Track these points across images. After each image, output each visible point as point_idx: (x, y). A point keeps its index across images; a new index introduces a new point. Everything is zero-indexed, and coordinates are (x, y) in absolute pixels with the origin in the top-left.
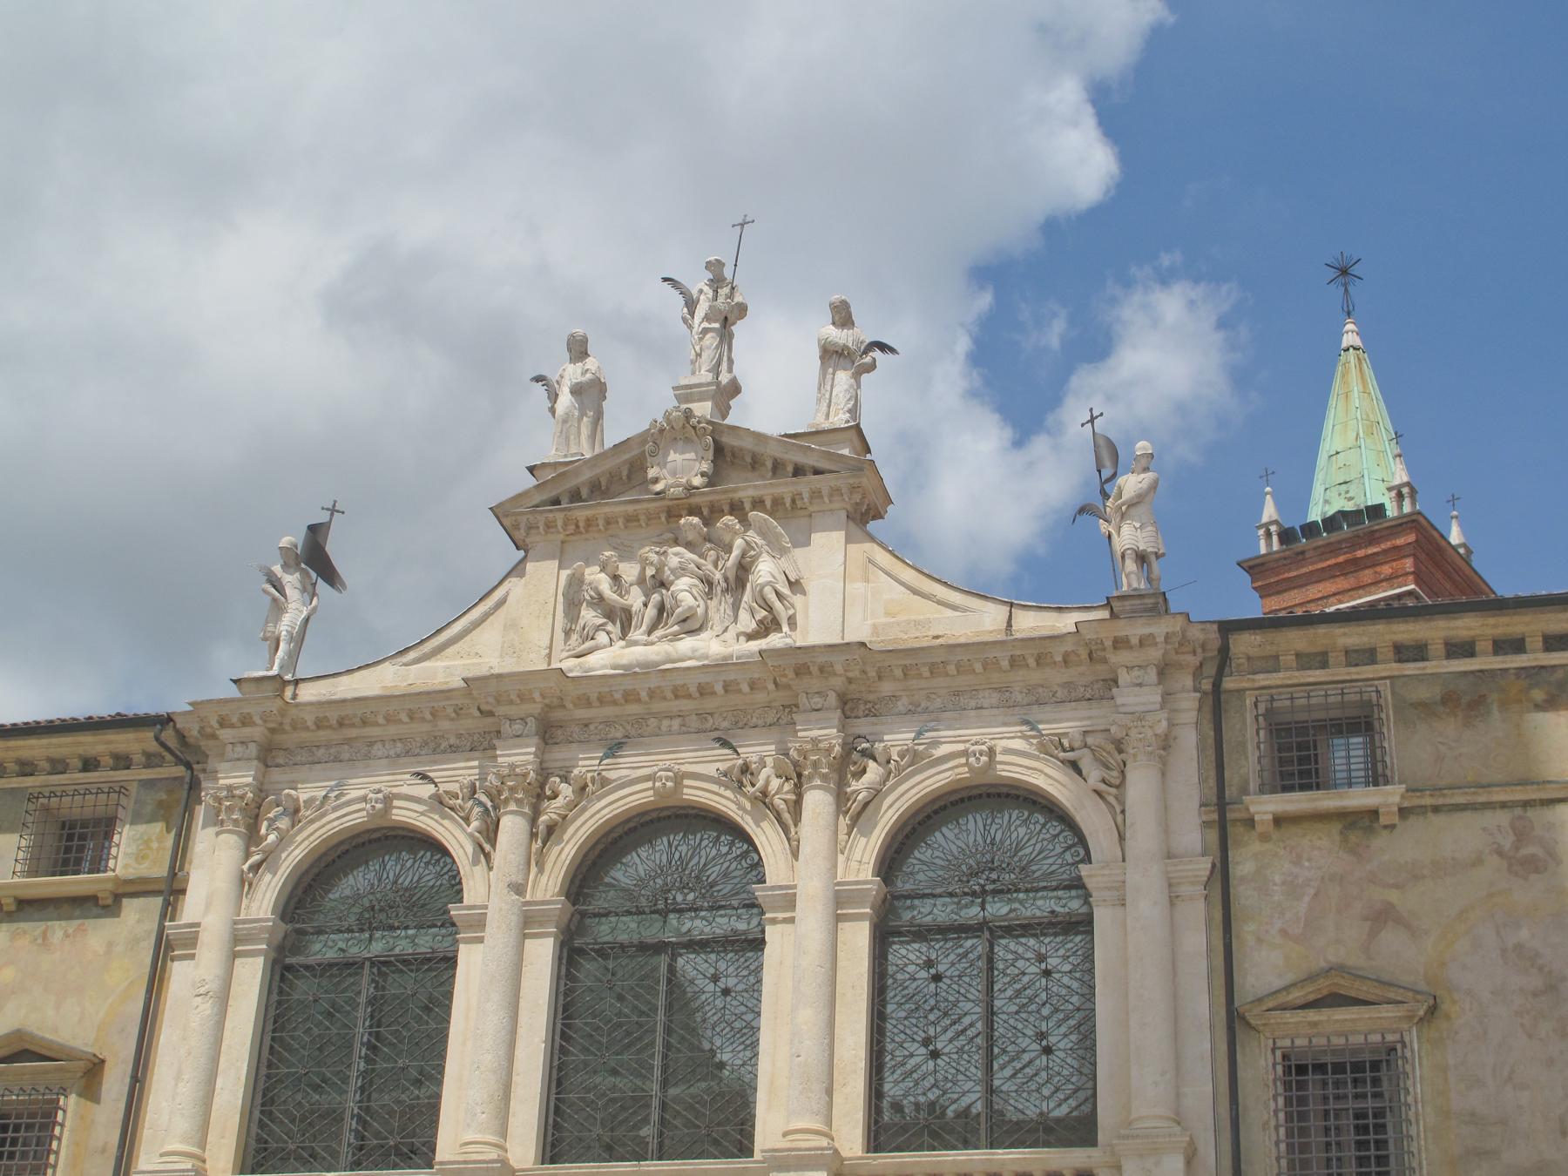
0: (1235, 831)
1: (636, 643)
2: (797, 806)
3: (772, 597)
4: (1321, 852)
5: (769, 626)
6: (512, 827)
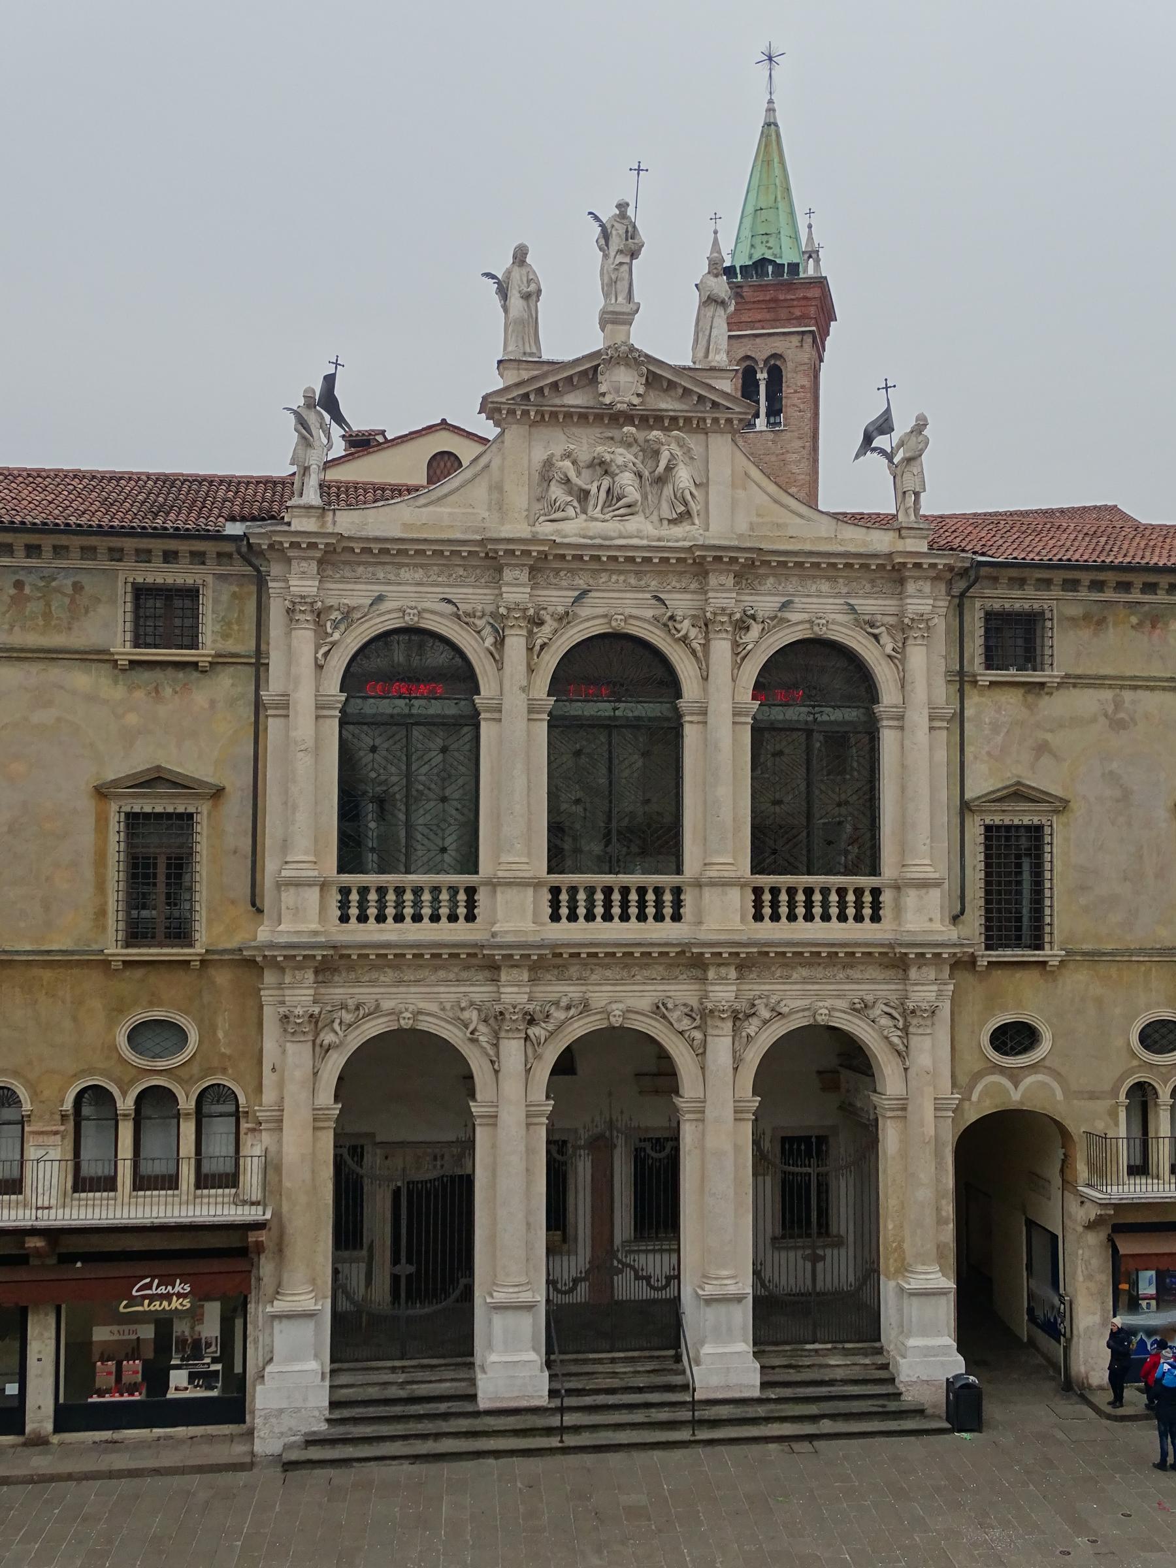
0: (967, 687)
1: (596, 519)
2: (706, 646)
3: (689, 497)
4: (1011, 700)
5: (685, 516)
6: (516, 644)
